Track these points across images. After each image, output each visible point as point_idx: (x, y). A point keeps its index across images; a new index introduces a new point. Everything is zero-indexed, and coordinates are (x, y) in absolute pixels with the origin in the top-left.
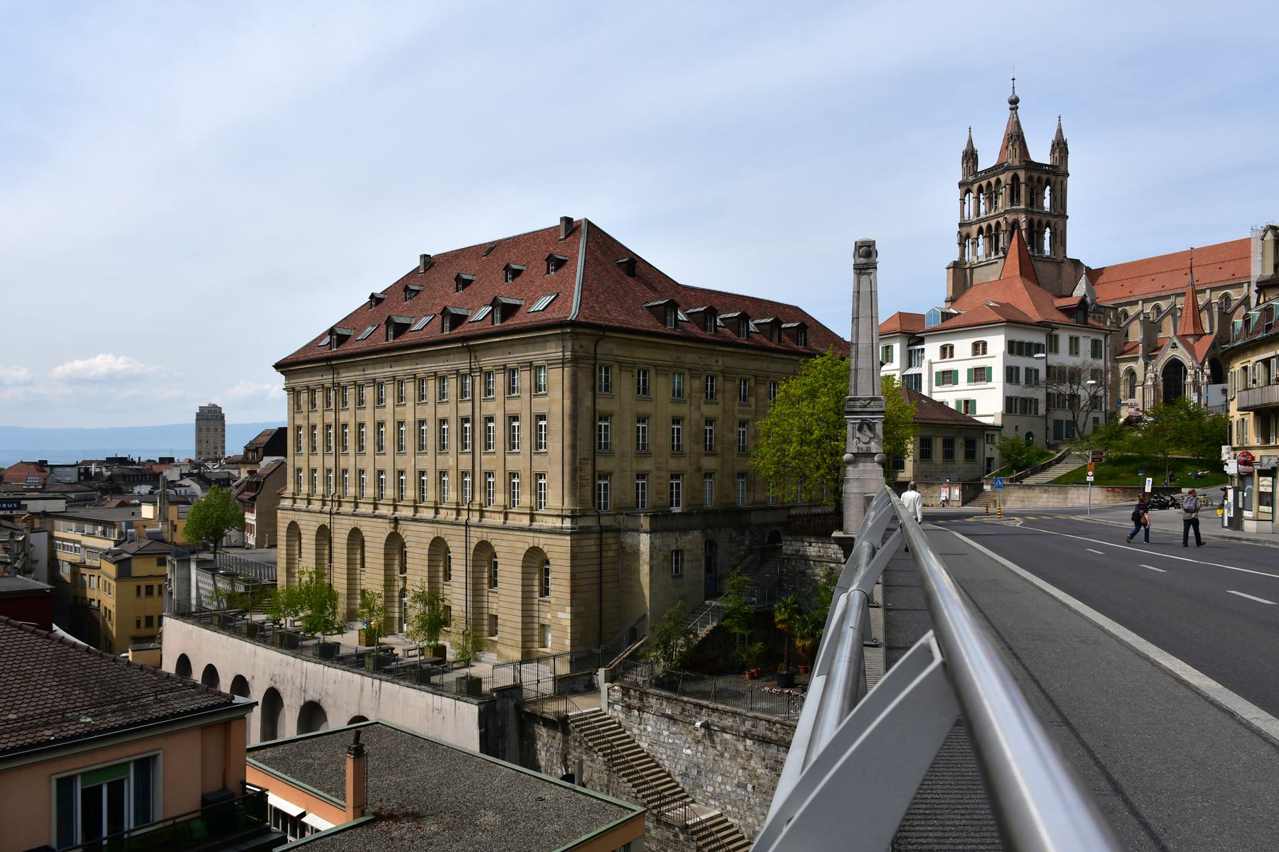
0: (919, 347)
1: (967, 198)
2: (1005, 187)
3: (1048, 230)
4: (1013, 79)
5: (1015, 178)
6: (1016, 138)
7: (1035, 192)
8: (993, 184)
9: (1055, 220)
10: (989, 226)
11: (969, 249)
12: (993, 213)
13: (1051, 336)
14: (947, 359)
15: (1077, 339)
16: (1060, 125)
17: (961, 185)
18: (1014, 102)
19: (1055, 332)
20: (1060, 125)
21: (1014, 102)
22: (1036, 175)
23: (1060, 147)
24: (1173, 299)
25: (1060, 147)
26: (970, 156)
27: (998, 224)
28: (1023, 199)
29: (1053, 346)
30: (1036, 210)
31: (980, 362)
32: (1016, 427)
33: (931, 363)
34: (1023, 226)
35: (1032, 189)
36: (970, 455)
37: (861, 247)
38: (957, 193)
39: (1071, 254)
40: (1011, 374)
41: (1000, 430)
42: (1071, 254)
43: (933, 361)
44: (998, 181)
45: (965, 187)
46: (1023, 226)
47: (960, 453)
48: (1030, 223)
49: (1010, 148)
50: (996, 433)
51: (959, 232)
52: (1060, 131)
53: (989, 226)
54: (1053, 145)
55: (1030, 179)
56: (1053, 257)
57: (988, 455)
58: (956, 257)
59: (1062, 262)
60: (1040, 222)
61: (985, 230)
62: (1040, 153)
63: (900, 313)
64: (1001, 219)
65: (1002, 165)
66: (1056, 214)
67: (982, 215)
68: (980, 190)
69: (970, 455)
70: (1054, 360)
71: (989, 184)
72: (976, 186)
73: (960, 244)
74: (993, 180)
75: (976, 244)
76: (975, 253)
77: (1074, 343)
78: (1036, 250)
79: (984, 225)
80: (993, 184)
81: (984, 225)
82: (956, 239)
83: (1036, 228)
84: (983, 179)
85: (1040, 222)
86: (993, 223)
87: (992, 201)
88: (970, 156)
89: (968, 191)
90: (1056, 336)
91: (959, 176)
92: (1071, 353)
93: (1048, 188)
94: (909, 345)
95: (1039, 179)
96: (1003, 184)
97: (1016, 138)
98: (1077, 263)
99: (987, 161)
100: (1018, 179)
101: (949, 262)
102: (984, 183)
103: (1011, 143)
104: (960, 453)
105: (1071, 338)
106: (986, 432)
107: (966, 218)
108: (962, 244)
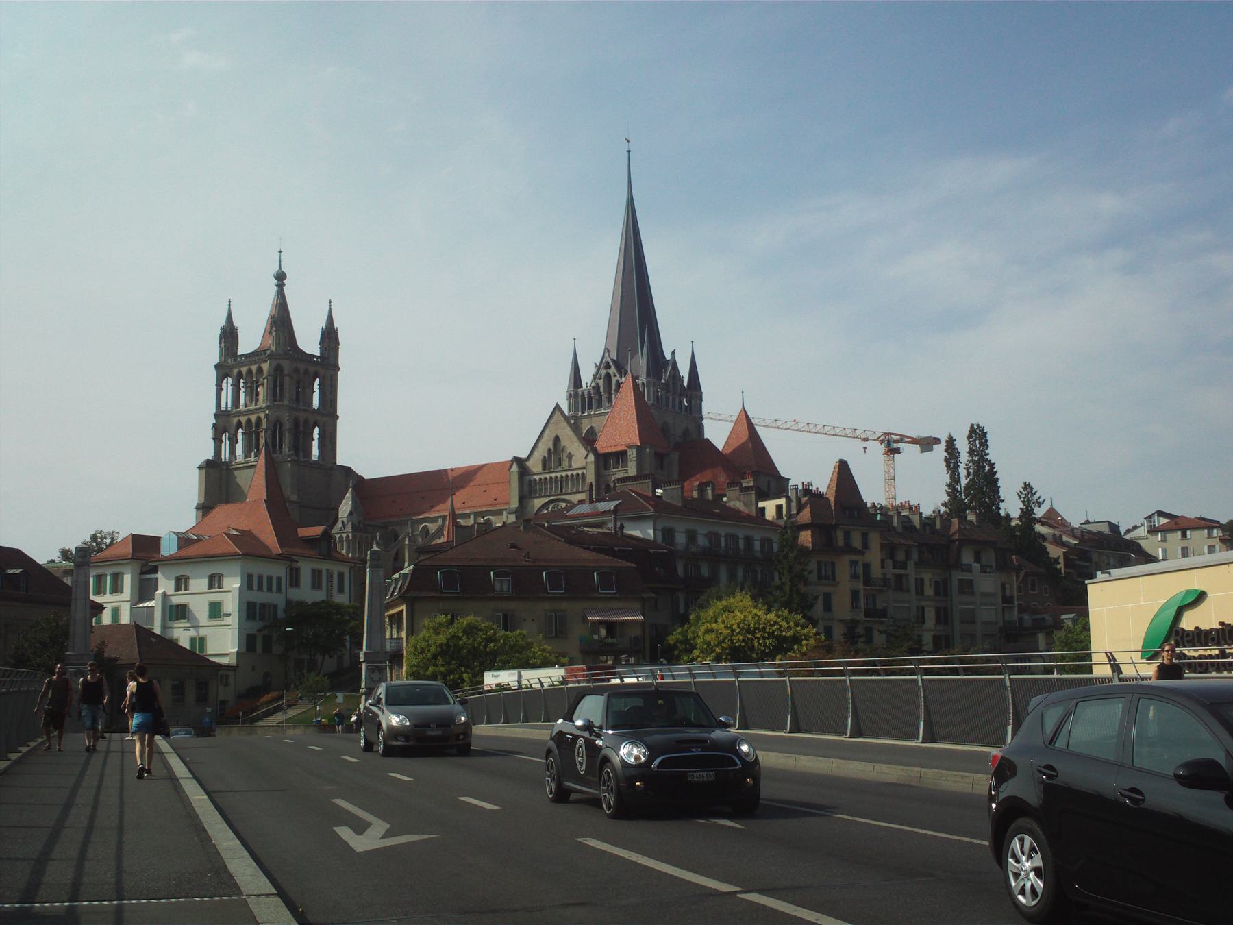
0: (153, 576)
1: (224, 385)
2: (267, 378)
3: (316, 430)
4: (280, 252)
5: (278, 371)
6: (281, 322)
7: (301, 386)
8: (254, 371)
9: (324, 419)
10: (249, 421)
11: (226, 446)
12: (253, 407)
13: (291, 570)
14: (183, 592)
15: (320, 572)
16: (330, 311)
17: (217, 367)
18: (281, 277)
19: (295, 565)
20: (330, 311)
21: (281, 277)
22: (302, 367)
23: (330, 337)
24: (440, 522)
25: (330, 337)
26: (229, 335)
27: (259, 419)
28: (287, 395)
29: (294, 579)
30: (302, 407)
31: (215, 597)
32: (253, 667)
33: (165, 595)
34: (287, 426)
35: (298, 383)
36: (202, 699)
37: (80, 551)
38: (213, 375)
39: (341, 460)
40: (250, 611)
41: (235, 670)
42: (341, 460)
43: (168, 593)
44: (260, 370)
45: (223, 371)
46: (287, 426)
47: (191, 694)
48: (296, 423)
49: (274, 333)
50: (231, 673)
51: (214, 425)
52: (330, 318)
53: (249, 421)
54: (323, 333)
55: (296, 370)
56: (321, 463)
57: (221, 697)
58: (210, 455)
59: (331, 469)
60: (306, 421)
61: (244, 425)
62: (309, 342)
63: (133, 536)
64: (262, 415)
65: (265, 351)
66: (325, 412)
67: (242, 407)
68: (240, 375)
69: (202, 699)
70: (296, 594)
71: (250, 371)
72: (235, 371)
73: (214, 439)
74: (254, 368)
75: (233, 441)
76: (232, 451)
77: (316, 574)
78: (301, 454)
79: (243, 419)
80: (254, 371)
81: (243, 419)
82: (210, 433)
83: (301, 429)
84: (243, 365)
85: (306, 421)
86: (253, 418)
87: (253, 395)
88: (229, 335)
89: (226, 376)
90: (298, 570)
91: (215, 357)
92: (313, 587)
93: (317, 381)
94: (142, 573)
95: (306, 372)
96: (265, 375)
97: (281, 322)
98: (348, 470)
99: (250, 340)
100: (282, 370)
101: (201, 460)
102: (244, 370)
103: (274, 329)
104: (191, 694)
105: (313, 571)
106: (220, 673)
107: (223, 409)
108: (218, 440)
